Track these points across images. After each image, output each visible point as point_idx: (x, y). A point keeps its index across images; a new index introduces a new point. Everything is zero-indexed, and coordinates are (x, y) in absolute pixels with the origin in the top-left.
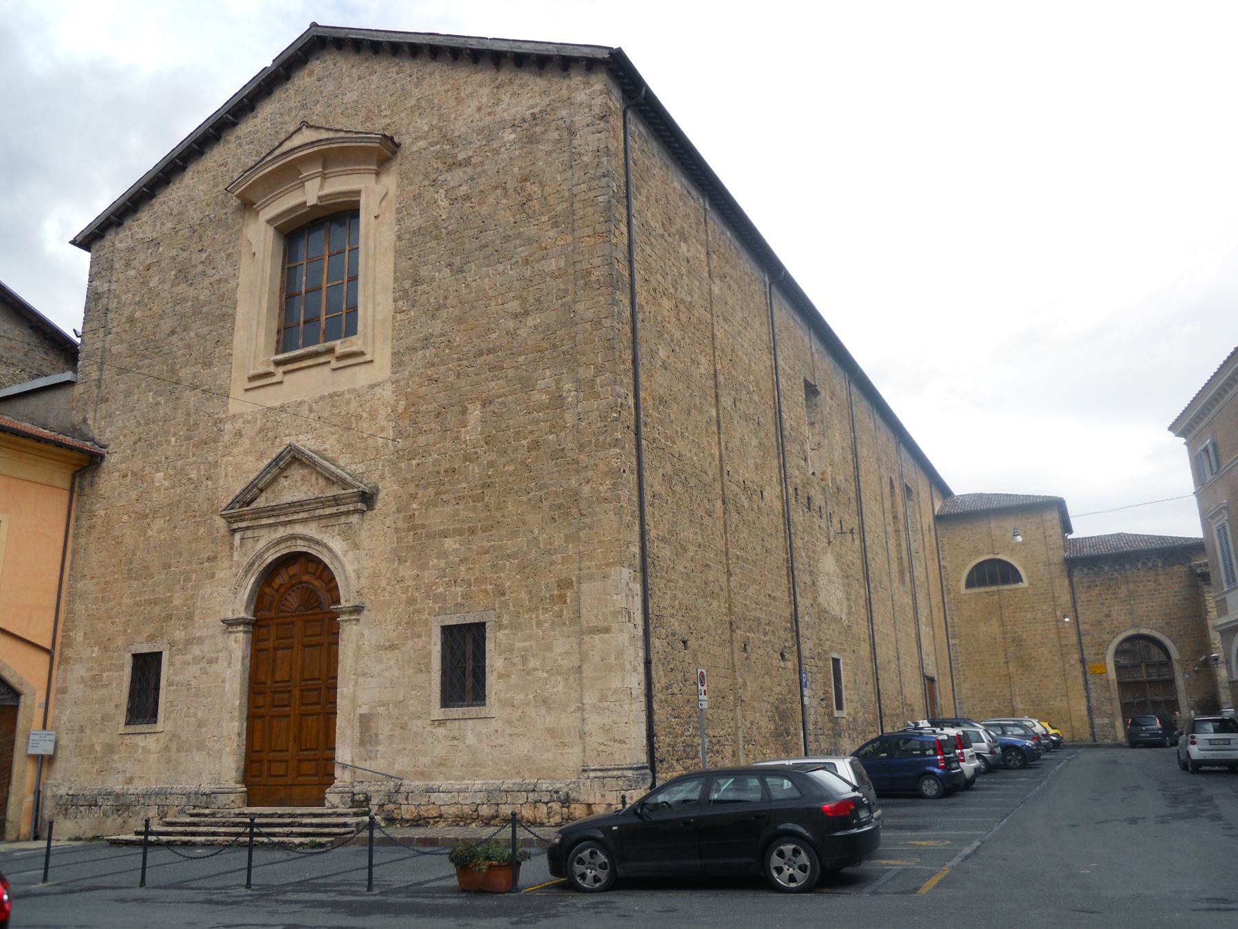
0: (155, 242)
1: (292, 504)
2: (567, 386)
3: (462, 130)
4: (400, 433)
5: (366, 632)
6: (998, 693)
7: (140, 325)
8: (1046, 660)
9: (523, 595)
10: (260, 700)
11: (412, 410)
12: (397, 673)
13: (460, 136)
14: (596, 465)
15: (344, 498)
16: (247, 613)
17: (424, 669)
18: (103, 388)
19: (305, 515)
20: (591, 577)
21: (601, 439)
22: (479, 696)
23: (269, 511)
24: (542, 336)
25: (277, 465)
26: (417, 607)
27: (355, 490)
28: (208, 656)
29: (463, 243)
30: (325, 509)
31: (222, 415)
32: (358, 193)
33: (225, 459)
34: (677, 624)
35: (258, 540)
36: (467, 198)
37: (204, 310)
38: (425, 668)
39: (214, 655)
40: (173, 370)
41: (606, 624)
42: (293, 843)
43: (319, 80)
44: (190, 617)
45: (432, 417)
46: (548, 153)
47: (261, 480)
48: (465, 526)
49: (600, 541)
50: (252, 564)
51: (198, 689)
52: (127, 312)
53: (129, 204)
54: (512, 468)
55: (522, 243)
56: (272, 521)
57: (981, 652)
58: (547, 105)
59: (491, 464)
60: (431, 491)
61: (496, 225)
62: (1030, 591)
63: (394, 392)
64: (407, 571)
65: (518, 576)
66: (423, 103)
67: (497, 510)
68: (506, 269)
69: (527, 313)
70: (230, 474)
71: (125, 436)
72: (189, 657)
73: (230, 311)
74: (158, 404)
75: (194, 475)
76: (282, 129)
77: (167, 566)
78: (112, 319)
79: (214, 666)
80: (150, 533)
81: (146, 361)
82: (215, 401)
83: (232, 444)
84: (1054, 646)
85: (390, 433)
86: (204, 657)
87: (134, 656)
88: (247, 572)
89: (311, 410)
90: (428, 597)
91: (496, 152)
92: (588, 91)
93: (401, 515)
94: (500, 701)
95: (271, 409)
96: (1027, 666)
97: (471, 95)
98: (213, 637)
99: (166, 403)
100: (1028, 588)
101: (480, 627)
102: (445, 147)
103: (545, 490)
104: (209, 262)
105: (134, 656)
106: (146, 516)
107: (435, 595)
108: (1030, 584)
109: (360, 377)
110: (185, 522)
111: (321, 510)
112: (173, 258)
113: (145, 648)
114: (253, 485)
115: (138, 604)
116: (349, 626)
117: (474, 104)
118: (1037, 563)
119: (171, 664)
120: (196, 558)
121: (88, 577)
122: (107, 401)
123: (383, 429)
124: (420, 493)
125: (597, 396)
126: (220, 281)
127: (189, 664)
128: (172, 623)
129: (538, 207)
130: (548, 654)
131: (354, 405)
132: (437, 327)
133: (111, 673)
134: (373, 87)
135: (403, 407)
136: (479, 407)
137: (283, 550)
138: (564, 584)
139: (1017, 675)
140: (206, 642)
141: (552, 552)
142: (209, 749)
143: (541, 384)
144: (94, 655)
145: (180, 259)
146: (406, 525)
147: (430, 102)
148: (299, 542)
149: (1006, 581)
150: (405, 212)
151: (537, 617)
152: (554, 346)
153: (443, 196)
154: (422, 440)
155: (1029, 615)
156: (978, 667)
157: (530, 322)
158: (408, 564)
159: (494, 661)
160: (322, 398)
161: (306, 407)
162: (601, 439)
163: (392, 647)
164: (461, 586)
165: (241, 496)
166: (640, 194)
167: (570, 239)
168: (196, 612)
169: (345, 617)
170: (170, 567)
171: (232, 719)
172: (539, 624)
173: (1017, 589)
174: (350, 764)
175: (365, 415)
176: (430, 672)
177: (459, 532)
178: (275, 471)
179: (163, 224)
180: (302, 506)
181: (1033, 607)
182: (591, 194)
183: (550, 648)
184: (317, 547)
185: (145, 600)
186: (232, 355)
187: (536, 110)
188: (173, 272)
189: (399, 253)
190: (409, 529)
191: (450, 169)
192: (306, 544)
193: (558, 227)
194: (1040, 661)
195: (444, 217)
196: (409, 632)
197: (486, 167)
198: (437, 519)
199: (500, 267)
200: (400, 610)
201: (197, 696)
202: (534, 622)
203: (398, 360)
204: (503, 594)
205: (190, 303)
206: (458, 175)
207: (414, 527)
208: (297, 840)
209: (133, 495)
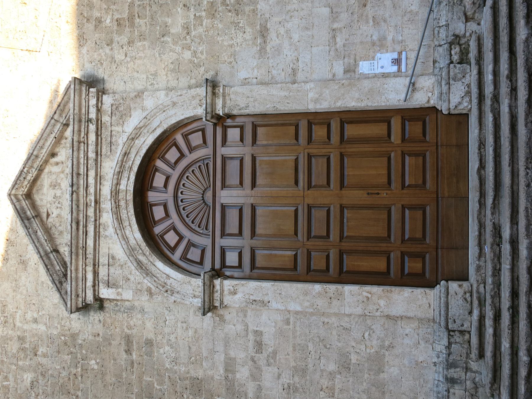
5: (243, 74)
10: (318, 263)
12: (296, 21)
15: (80, 109)
19: (92, 173)
23: (78, 229)
25: (28, 219)
27: (72, 86)
28: (251, 351)
30: (90, 142)
33: (18, 324)
35: (113, 258)
47: (42, 245)
50: (140, 265)
51: (296, 370)
56: (91, 229)
75: (28, 377)
93: (116, 38)
111: (90, 147)
114: (45, 257)
116: (232, 96)
120: (124, 375)
140: (232, 354)
142: (382, 347)
146: (127, 29)
148: (122, 187)
158: (169, 21)
163: (264, 33)
165: (55, 276)
168: (193, 374)
169: (219, 103)
171: (340, 295)
174: (408, 79)
178: (36, 224)
184: (132, 156)
200: (221, 26)
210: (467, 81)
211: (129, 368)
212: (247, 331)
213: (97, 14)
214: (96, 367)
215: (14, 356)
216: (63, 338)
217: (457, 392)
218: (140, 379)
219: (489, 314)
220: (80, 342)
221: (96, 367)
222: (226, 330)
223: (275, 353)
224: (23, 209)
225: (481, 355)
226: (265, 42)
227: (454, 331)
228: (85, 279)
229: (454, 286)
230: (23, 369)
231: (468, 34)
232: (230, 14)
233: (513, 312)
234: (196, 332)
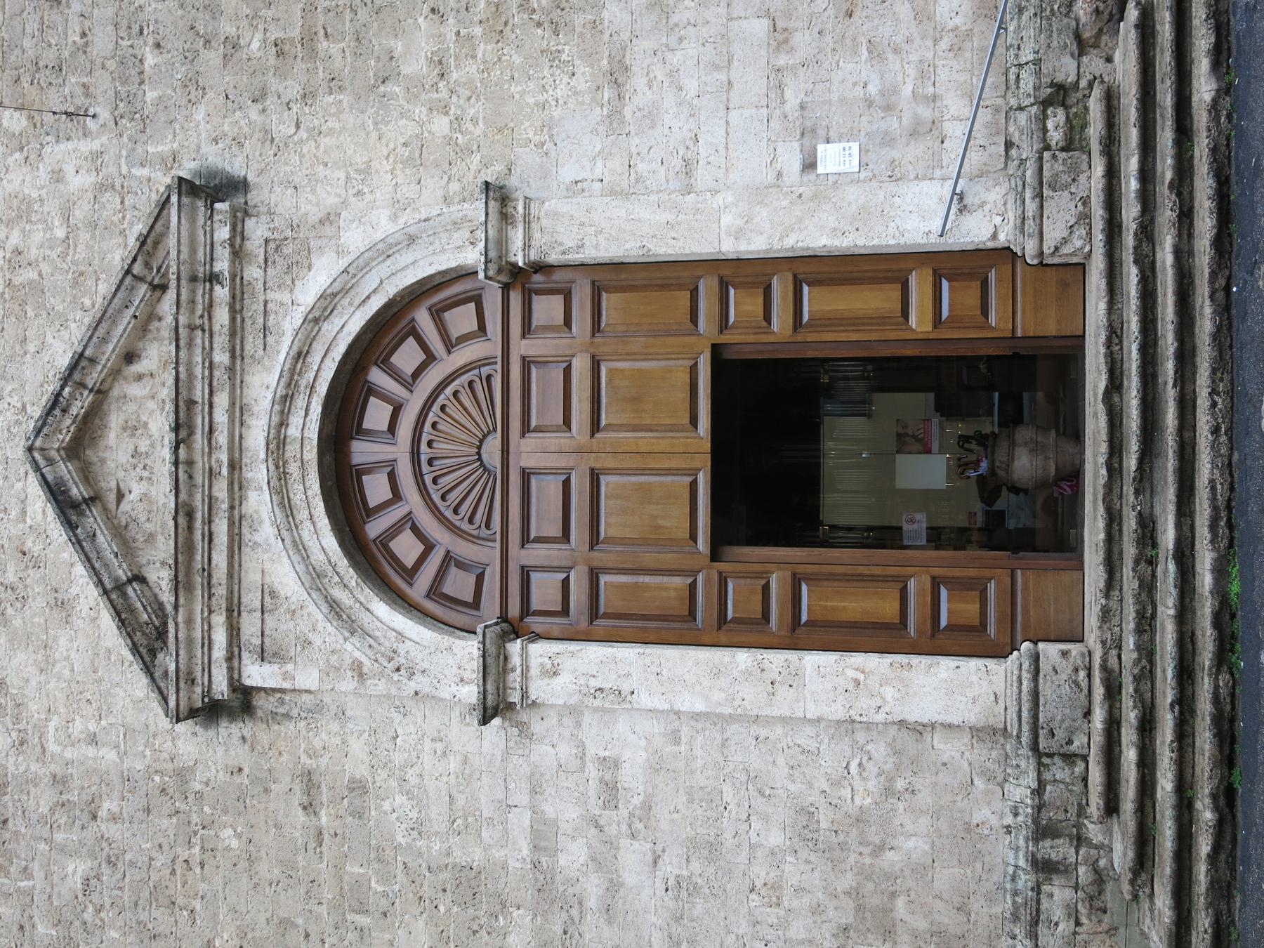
5: (568, 173)
12: (691, 49)
15: (193, 251)
19: (222, 400)
23: (190, 528)
27: (174, 199)
30: (216, 328)
33: (53, 747)
35: (273, 594)
42: (1214, 106)
50: (335, 608)
56: (221, 527)
72: (593, 889)
75: (77, 869)
83: (17, 720)
110: (198, 905)
111: (216, 339)
140: (549, 810)
148: (293, 431)
158: (399, 46)
163: (617, 75)
165: (138, 636)
168: (458, 856)
169: (517, 237)
184: (315, 359)
200: (517, 59)
201: (713, 849)
208: (1204, 88)
210: (1080, 189)
211: (312, 845)
212: (582, 758)
213: (228, 29)
214: (235, 844)
215: (42, 820)
216: (157, 778)
217: (1056, 891)
218: (338, 869)
219: (1130, 716)
220: (198, 787)
221: (235, 844)
222: (534, 758)
223: (647, 807)
224: (61, 482)
225: (1111, 807)
227: (1051, 755)
228: (208, 643)
229: (1050, 651)
231: (1083, 83)
232: (539, 31)
233: (1181, 713)
234: (465, 760)
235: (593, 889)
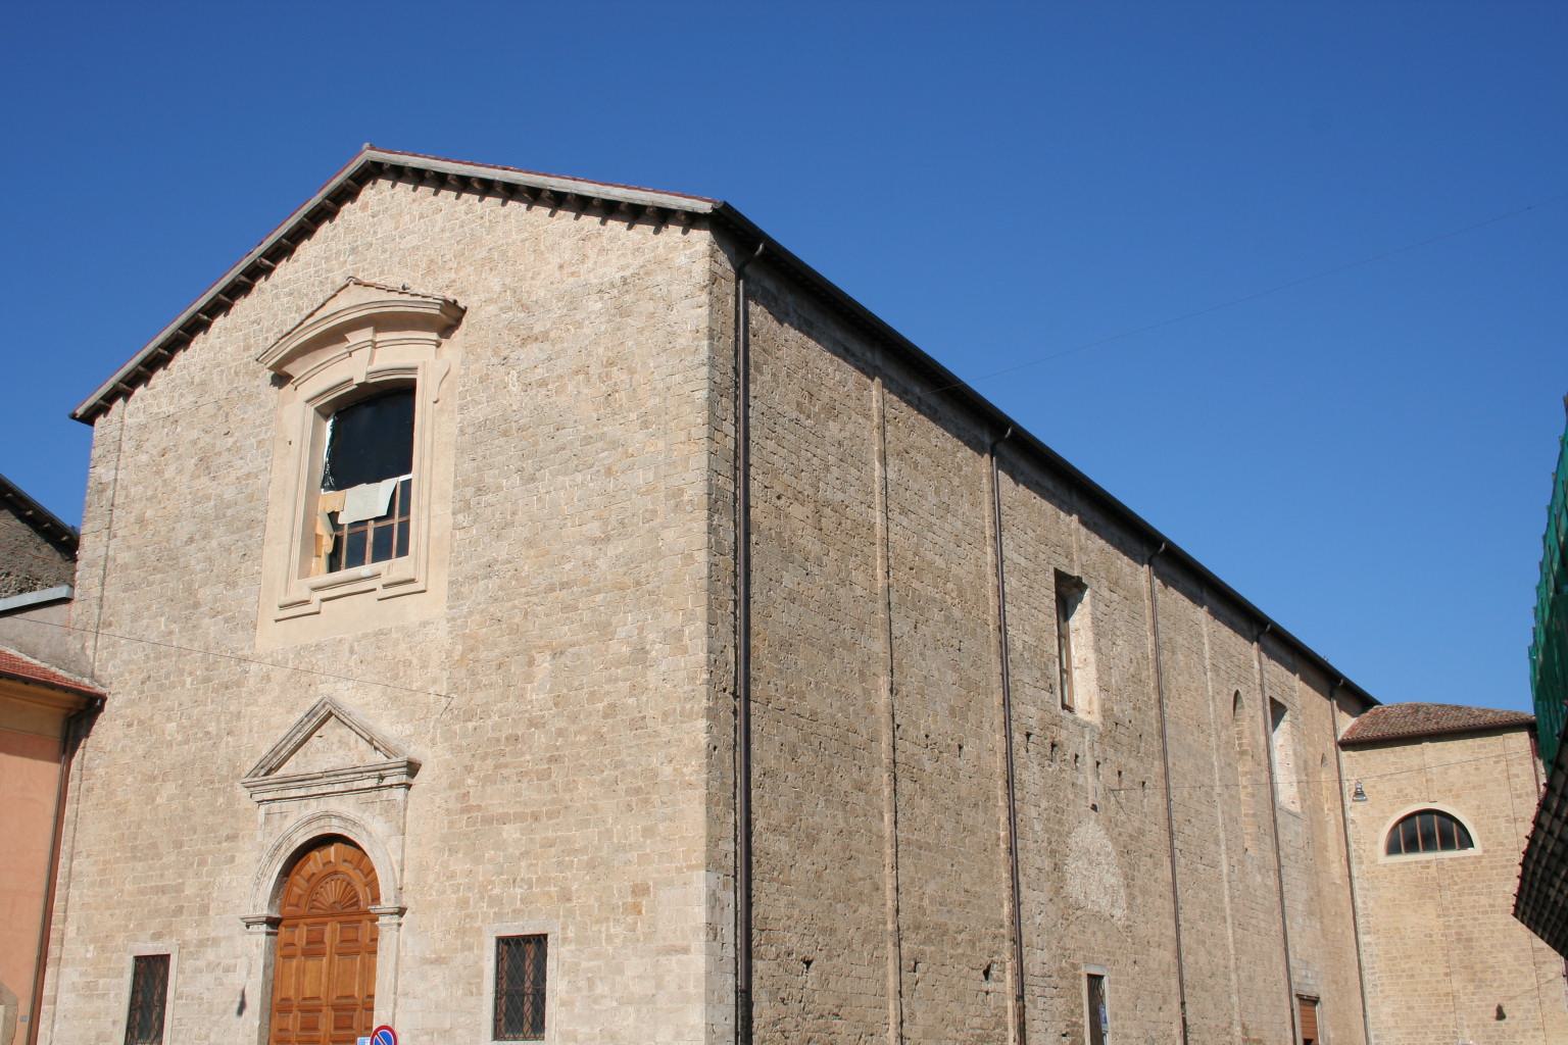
0: (171, 419)
1: (326, 774)
2: (651, 637)
3: (542, 293)
4: (455, 687)
6: (1435, 1023)
7: (151, 527)
8: (1510, 972)
9: (592, 901)
11: (471, 656)
13: (536, 302)
14: (681, 740)
16: (272, 910)
17: (474, 990)
18: (105, 609)
20: (670, 883)
21: (688, 706)
22: (538, 1027)
24: (625, 569)
26: (470, 910)
29: (536, 443)
31: (247, 652)
32: (414, 369)
34: (795, 939)
35: (286, 816)
36: (543, 383)
37: (229, 512)
38: (473, 990)
39: (233, 961)
40: (190, 590)
41: (685, 943)
43: (373, 217)
44: (204, 910)
45: (494, 667)
46: (641, 331)
48: (528, 811)
49: (682, 837)
52: (137, 507)
53: (141, 368)
54: (583, 738)
55: (605, 447)
57: (1410, 957)
58: (642, 267)
59: (560, 733)
60: (490, 763)
61: (576, 422)
62: (1484, 862)
63: (450, 632)
64: (459, 865)
65: (588, 877)
66: (496, 255)
67: (564, 790)
68: (585, 480)
69: (608, 539)
70: (255, 729)
71: (131, 673)
72: (201, 963)
73: (260, 516)
74: (171, 633)
75: (212, 728)
76: (327, 278)
77: (179, 845)
78: (117, 517)
79: (231, 975)
80: (159, 800)
81: (159, 576)
82: (240, 633)
84: (1523, 950)
85: (444, 688)
86: (219, 964)
87: (138, 959)
88: (272, 857)
89: (352, 651)
90: (482, 898)
91: (579, 325)
92: (688, 252)
93: (454, 793)
94: (561, 1034)
95: (305, 648)
96: (1481, 980)
97: (552, 248)
98: (230, 938)
99: (180, 632)
100: (1481, 857)
101: (541, 940)
102: (519, 315)
103: (621, 770)
104: (236, 449)
105: (138, 959)
106: (153, 778)
107: (490, 897)
108: (1485, 851)
109: (412, 609)
110: (201, 788)
112: (194, 443)
113: (150, 949)
115: (142, 892)
117: (555, 260)
118: (1496, 817)
119: (181, 971)
121: (84, 854)
122: (110, 625)
123: (435, 681)
124: (477, 764)
125: (685, 651)
126: (248, 475)
127: (201, 971)
128: (183, 917)
129: (624, 400)
130: (618, 978)
131: (403, 646)
132: (502, 550)
133: (109, 980)
134: (437, 229)
135: (459, 653)
136: (549, 658)
137: (315, 831)
138: (641, 890)
139: (1466, 994)
140: (223, 944)
141: (627, 848)
143: (621, 633)
144: (88, 956)
145: (201, 444)
147: (504, 253)
148: (334, 821)
149: (1447, 843)
150: (469, 398)
151: (608, 929)
152: (638, 583)
153: (515, 379)
154: (480, 697)
155: (1484, 900)
156: (1404, 980)
157: (616, 548)
158: (460, 855)
159: (556, 985)
160: (365, 636)
161: (346, 647)
162: (688, 706)
163: (438, 961)
164: (521, 887)
166: (762, 374)
167: (661, 444)
168: (212, 906)
170: (181, 847)
172: (609, 939)
173: (1464, 858)
175: (415, 661)
176: (481, 994)
177: (519, 817)
179: (182, 395)
180: (337, 775)
181: (1490, 886)
182: (688, 388)
183: (620, 971)
185: (151, 887)
186: (260, 573)
187: (627, 273)
188: (193, 461)
189: (461, 451)
190: (463, 811)
191: (524, 342)
192: (342, 824)
193: (647, 428)
194: (1500, 972)
195: (515, 408)
196: (459, 942)
197: (565, 345)
198: (495, 800)
199: (579, 477)
202: (604, 935)
203: (456, 596)
204: (569, 900)
205: (212, 503)
206: (534, 351)
207: (467, 810)
209: (140, 750)
226: (432, 963)
230: (218, 721)
235: (201, 963)
